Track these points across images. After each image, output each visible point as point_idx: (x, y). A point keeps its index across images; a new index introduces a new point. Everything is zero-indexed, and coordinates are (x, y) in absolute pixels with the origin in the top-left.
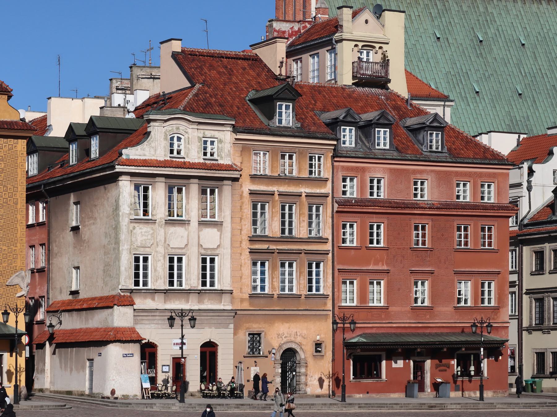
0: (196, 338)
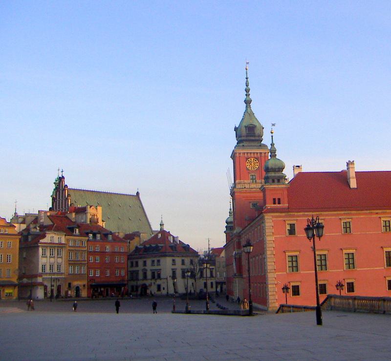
0: (55, 284)
